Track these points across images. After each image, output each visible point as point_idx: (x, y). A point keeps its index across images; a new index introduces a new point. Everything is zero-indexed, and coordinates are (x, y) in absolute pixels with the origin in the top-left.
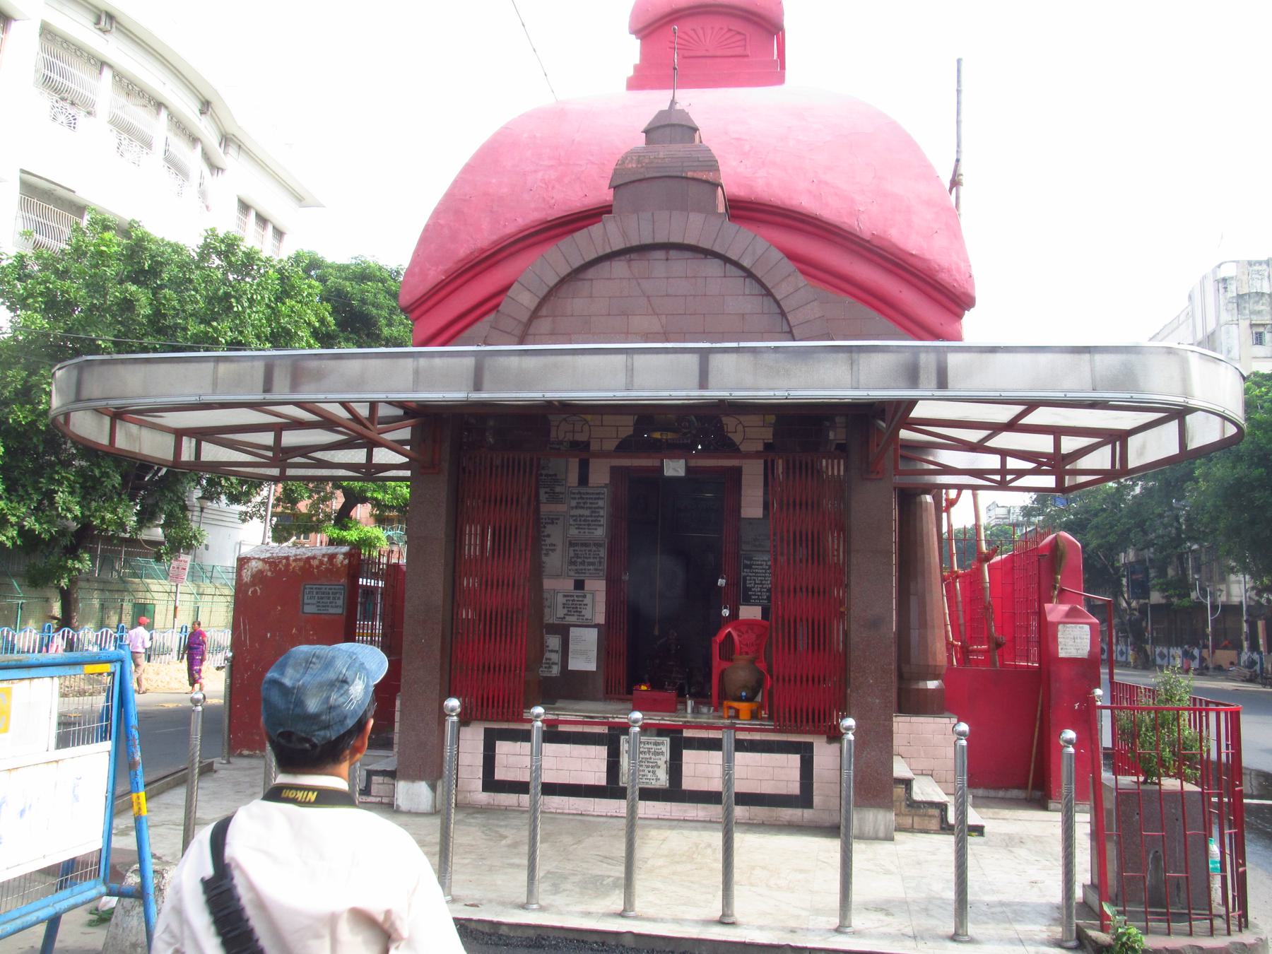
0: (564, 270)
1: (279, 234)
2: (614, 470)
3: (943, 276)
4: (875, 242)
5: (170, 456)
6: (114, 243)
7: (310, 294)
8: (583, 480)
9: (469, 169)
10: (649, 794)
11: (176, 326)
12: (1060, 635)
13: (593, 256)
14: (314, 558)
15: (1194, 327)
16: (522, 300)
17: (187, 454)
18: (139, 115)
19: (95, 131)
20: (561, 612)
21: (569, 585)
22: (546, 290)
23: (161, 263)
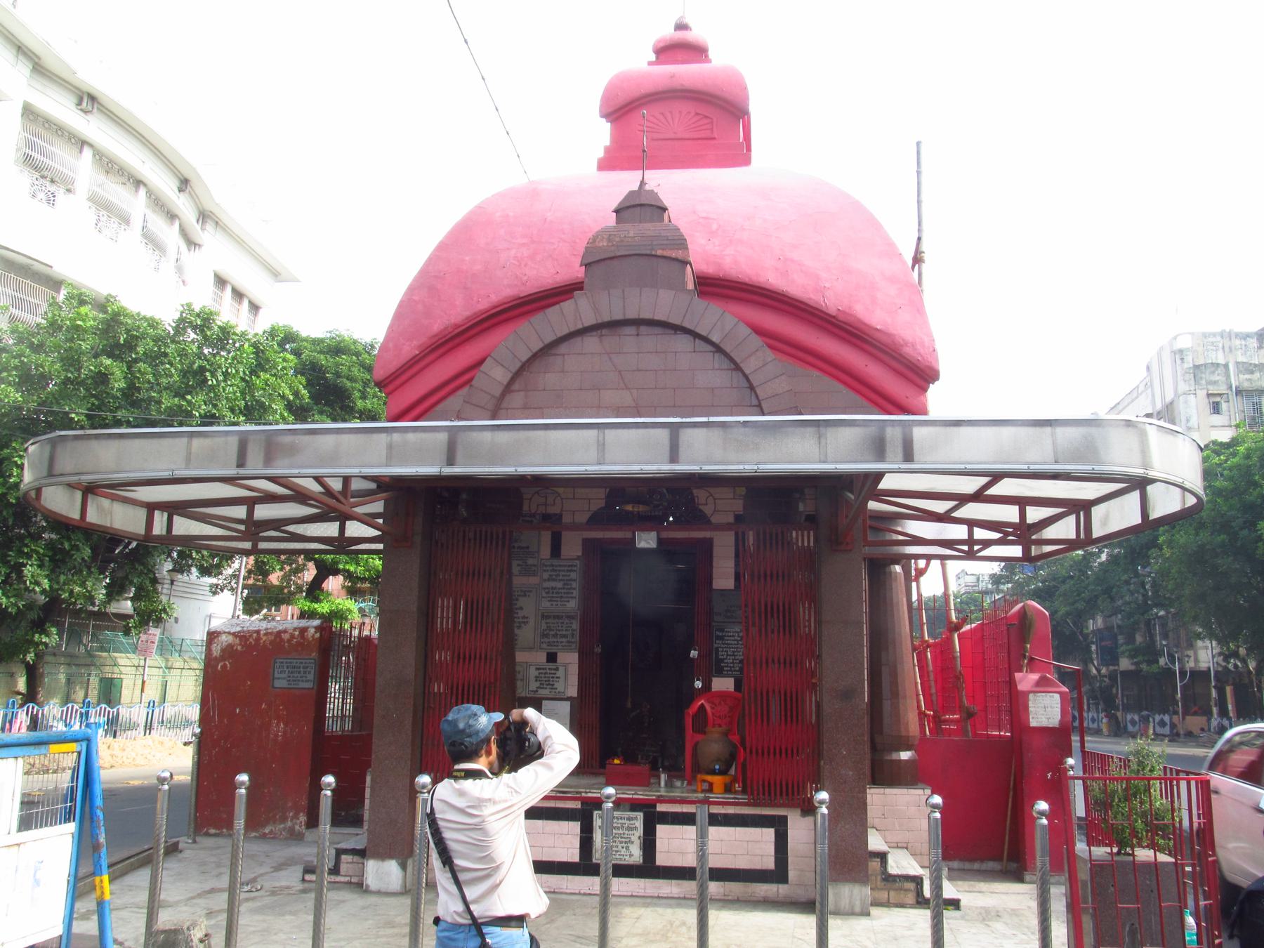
0: (536, 346)
1: (255, 308)
2: (586, 542)
3: (908, 350)
4: (841, 317)
5: (141, 529)
6: (90, 317)
7: (284, 368)
9: (442, 247)
10: (622, 871)
11: (150, 399)
12: (1031, 704)
13: (565, 331)
14: (285, 631)
15: (1153, 396)
16: (495, 374)
17: (159, 528)
18: (118, 193)
19: (74, 209)
20: (534, 685)
21: (542, 657)
22: (518, 365)
23: (137, 337)
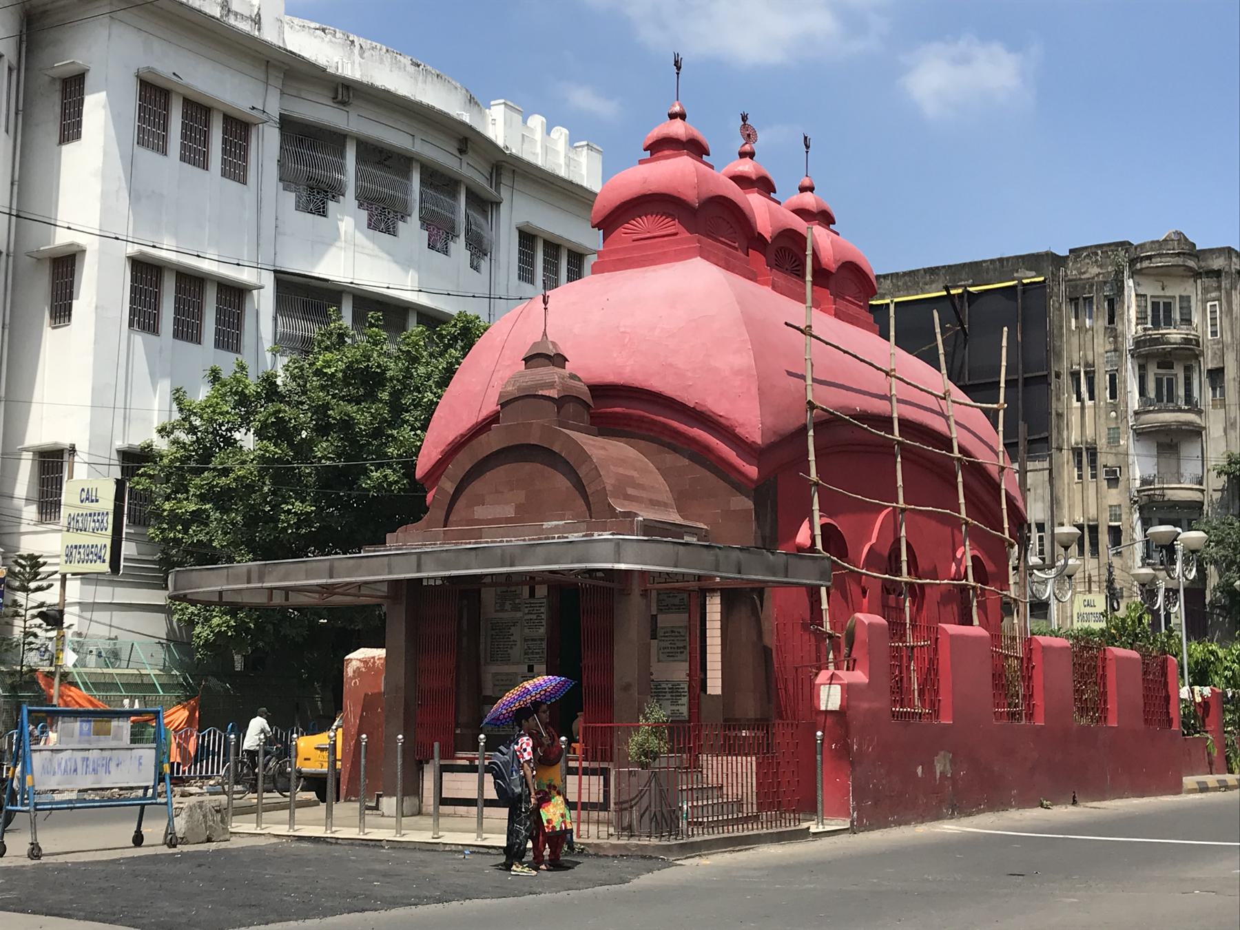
8: (532, 594)
